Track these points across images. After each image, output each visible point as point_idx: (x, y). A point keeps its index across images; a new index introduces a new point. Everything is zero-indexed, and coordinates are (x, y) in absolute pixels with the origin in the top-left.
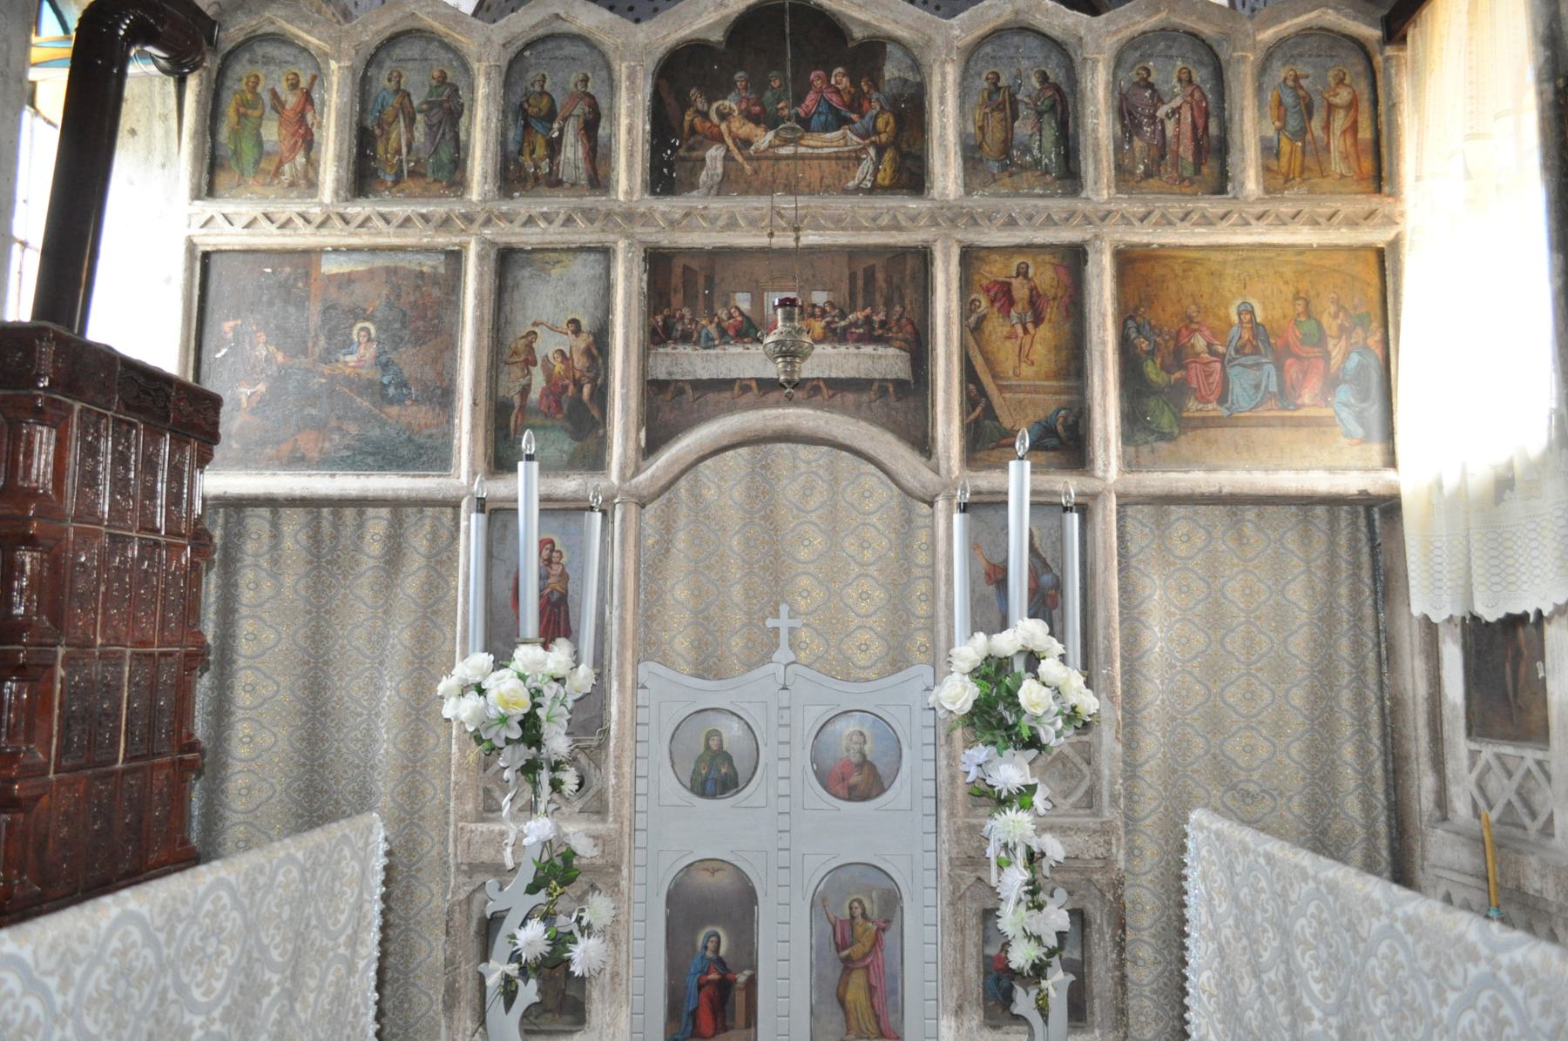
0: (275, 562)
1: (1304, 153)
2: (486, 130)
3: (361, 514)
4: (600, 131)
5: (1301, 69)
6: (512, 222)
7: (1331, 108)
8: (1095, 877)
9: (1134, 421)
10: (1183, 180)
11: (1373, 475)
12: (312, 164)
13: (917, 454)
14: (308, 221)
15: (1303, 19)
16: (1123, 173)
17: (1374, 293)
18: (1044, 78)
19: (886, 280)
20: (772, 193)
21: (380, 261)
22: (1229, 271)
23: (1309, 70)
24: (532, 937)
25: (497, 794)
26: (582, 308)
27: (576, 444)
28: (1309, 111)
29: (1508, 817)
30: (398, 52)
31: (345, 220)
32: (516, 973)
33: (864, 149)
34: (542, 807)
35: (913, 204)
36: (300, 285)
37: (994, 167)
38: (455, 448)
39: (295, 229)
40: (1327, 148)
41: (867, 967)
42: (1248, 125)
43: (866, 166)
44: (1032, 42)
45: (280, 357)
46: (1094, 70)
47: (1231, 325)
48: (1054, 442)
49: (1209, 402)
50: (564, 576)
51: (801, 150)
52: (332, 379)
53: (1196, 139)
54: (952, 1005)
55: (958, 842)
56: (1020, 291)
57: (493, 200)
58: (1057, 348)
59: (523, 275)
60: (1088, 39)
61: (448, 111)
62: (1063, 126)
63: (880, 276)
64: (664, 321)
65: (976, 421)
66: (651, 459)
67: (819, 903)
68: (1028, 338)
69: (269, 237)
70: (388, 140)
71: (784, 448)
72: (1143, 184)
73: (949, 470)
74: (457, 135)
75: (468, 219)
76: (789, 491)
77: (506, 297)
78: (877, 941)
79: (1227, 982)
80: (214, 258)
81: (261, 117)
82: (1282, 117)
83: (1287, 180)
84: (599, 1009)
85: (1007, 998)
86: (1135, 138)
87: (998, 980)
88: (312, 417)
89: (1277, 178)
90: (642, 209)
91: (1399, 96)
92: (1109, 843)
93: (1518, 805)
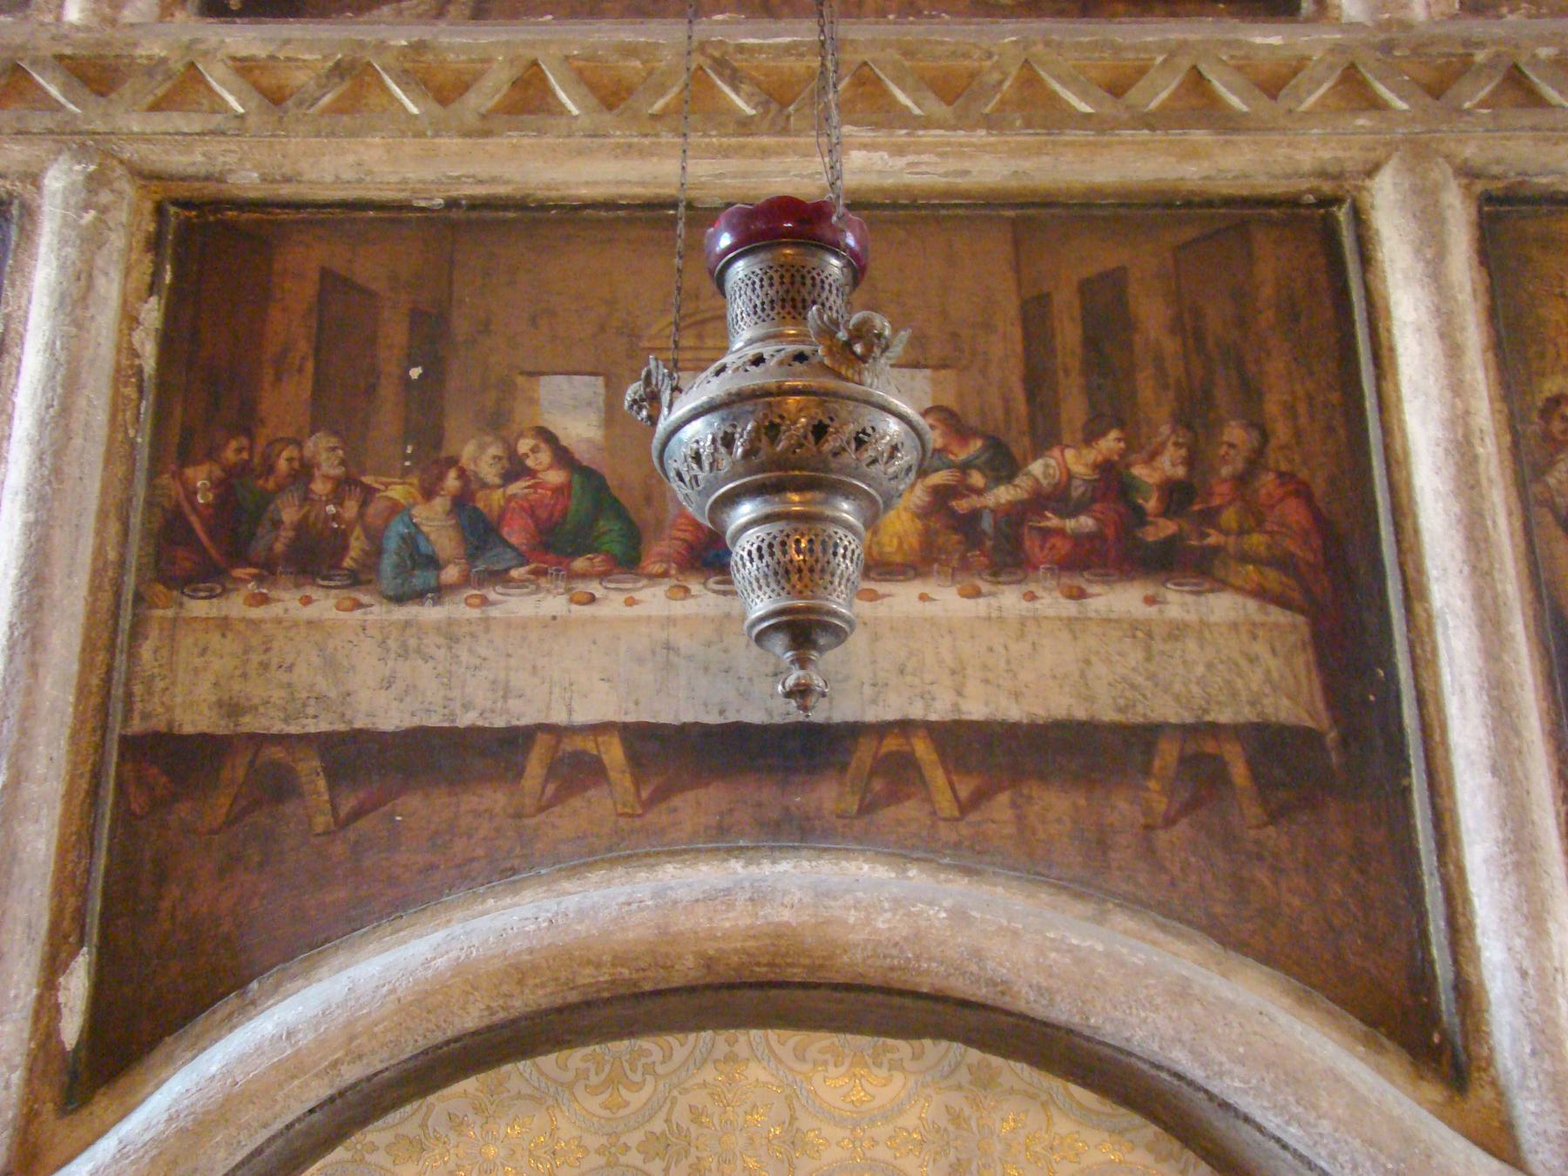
19: (1176, 327)
63: (1152, 315)
64: (225, 487)
66: (102, 1104)
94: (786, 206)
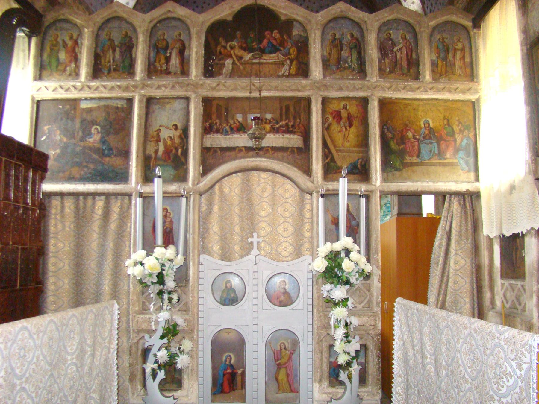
0: (62, 217)
1: (446, 66)
2: (142, 53)
3: (94, 199)
4: (186, 54)
5: (445, 35)
6: (152, 88)
7: (455, 50)
8: (370, 332)
9: (386, 164)
10: (403, 74)
11: (471, 184)
12: (78, 67)
13: (305, 176)
14: (76, 88)
15: (445, 18)
16: (382, 71)
17: (471, 118)
18: (352, 35)
19: (294, 110)
20: (251, 76)
21: (102, 103)
22: (420, 108)
23: (448, 36)
24: (163, 355)
25: (147, 304)
26: (177, 119)
27: (176, 172)
28: (448, 51)
29: (513, 307)
30: (110, 25)
31: (89, 88)
32: (157, 368)
33: (285, 60)
34: (165, 308)
35: (304, 82)
36: (73, 112)
37: (334, 68)
38: (130, 173)
39: (71, 91)
40: (455, 63)
41: (286, 367)
42: (426, 55)
43: (286, 67)
44: (348, 22)
45: (65, 140)
46: (371, 33)
47: (421, 128)
48: (357, 171)
49: (413, 157)
50: (171, 222)
51: (262, 61)
52: (84, 147)
53: (408, 60)
54: (318, 379)
55: (320, 320)
56: (344, 114)
57: (145, 79)
58: (358, 136)
59: (155, 107)
60: (368, 22)
61: (128, 47)
62: (359, 53)
63: (292, 109)
64: (210, 125)
65: (328, 163)
66: (205, 177)
67: (268, 344)
68: (347, 132)
69: (62, 95)
70: (106, 57)
71: (255, 173)
72: (389, 75)
73: (318, 182)
74: (131, 55)
75: (135, 87)
76: (257, 190)
77: (149, 116)
78: (290, 358)
79: (405, 354)
80: (41, 102)
81: (59, 50)
82: (438, 53)
83: (441, 75)
84: (186, 382)
85: (338, 375)
86: (386, 59)
87: (334, 370)
88: (77, 162)
89: (437, 75)
90: (201, 83)
91: (479, 47)
92: (375, 320)
93: (515, 301)
94: (256, 117)
